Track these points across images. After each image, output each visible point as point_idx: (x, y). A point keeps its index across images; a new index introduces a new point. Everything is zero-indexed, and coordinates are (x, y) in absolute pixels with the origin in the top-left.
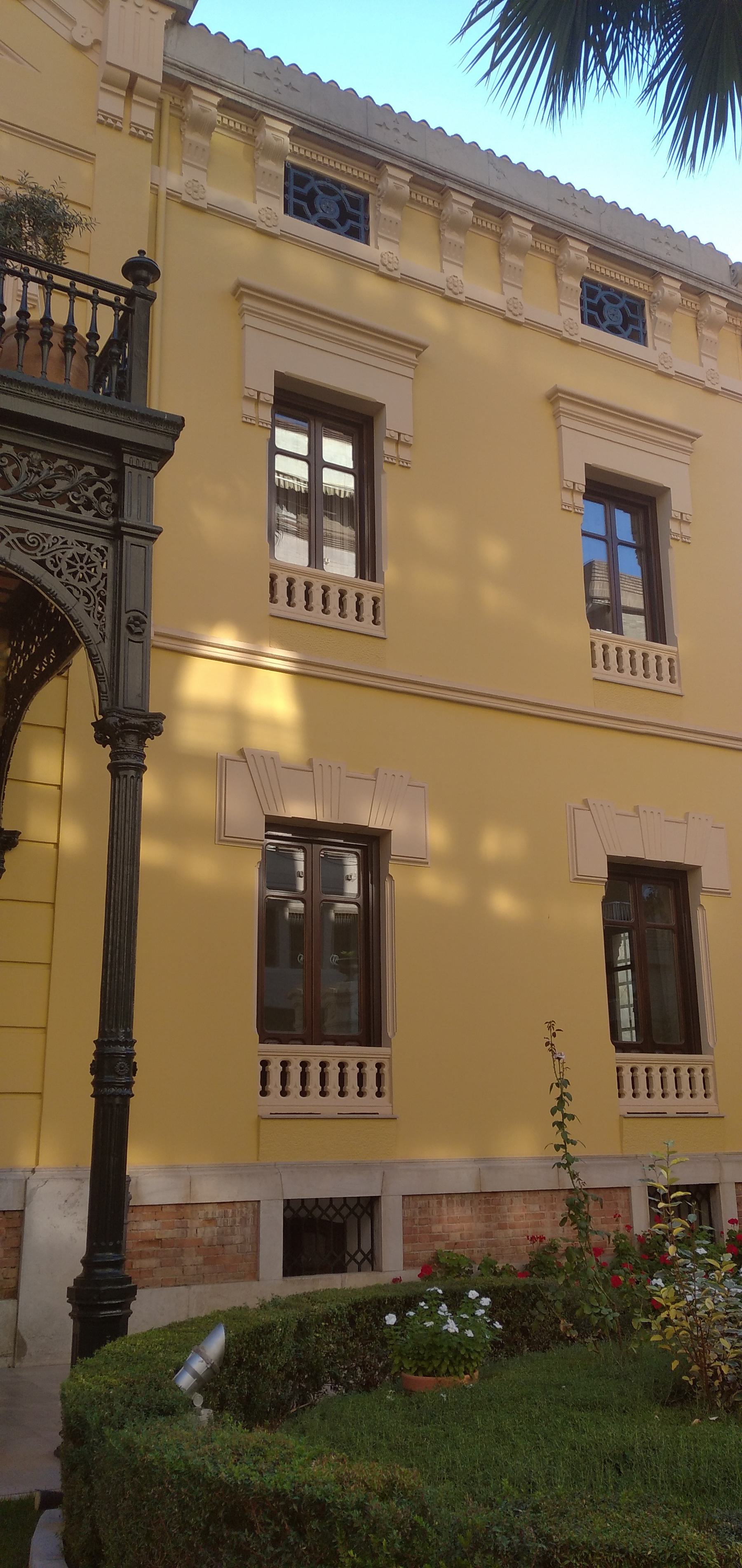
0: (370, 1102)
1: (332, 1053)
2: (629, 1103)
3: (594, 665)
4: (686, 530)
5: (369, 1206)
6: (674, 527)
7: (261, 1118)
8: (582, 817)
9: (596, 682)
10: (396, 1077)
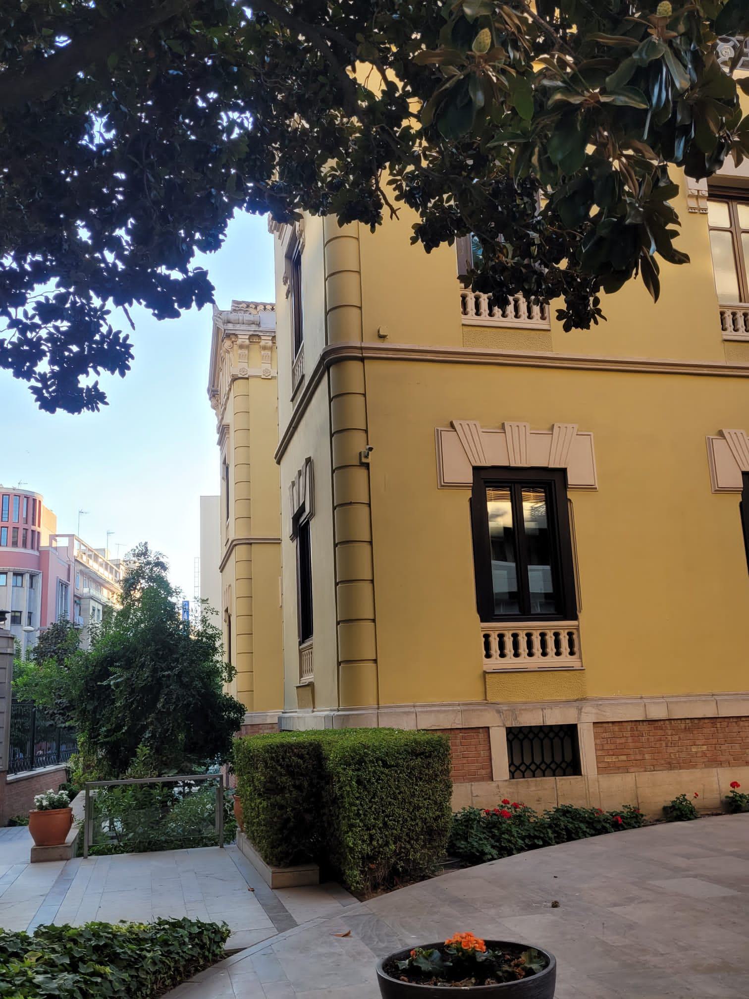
7: (485, 673)
8: (719, 444)
9: (726, 343)
10: (585, 641)
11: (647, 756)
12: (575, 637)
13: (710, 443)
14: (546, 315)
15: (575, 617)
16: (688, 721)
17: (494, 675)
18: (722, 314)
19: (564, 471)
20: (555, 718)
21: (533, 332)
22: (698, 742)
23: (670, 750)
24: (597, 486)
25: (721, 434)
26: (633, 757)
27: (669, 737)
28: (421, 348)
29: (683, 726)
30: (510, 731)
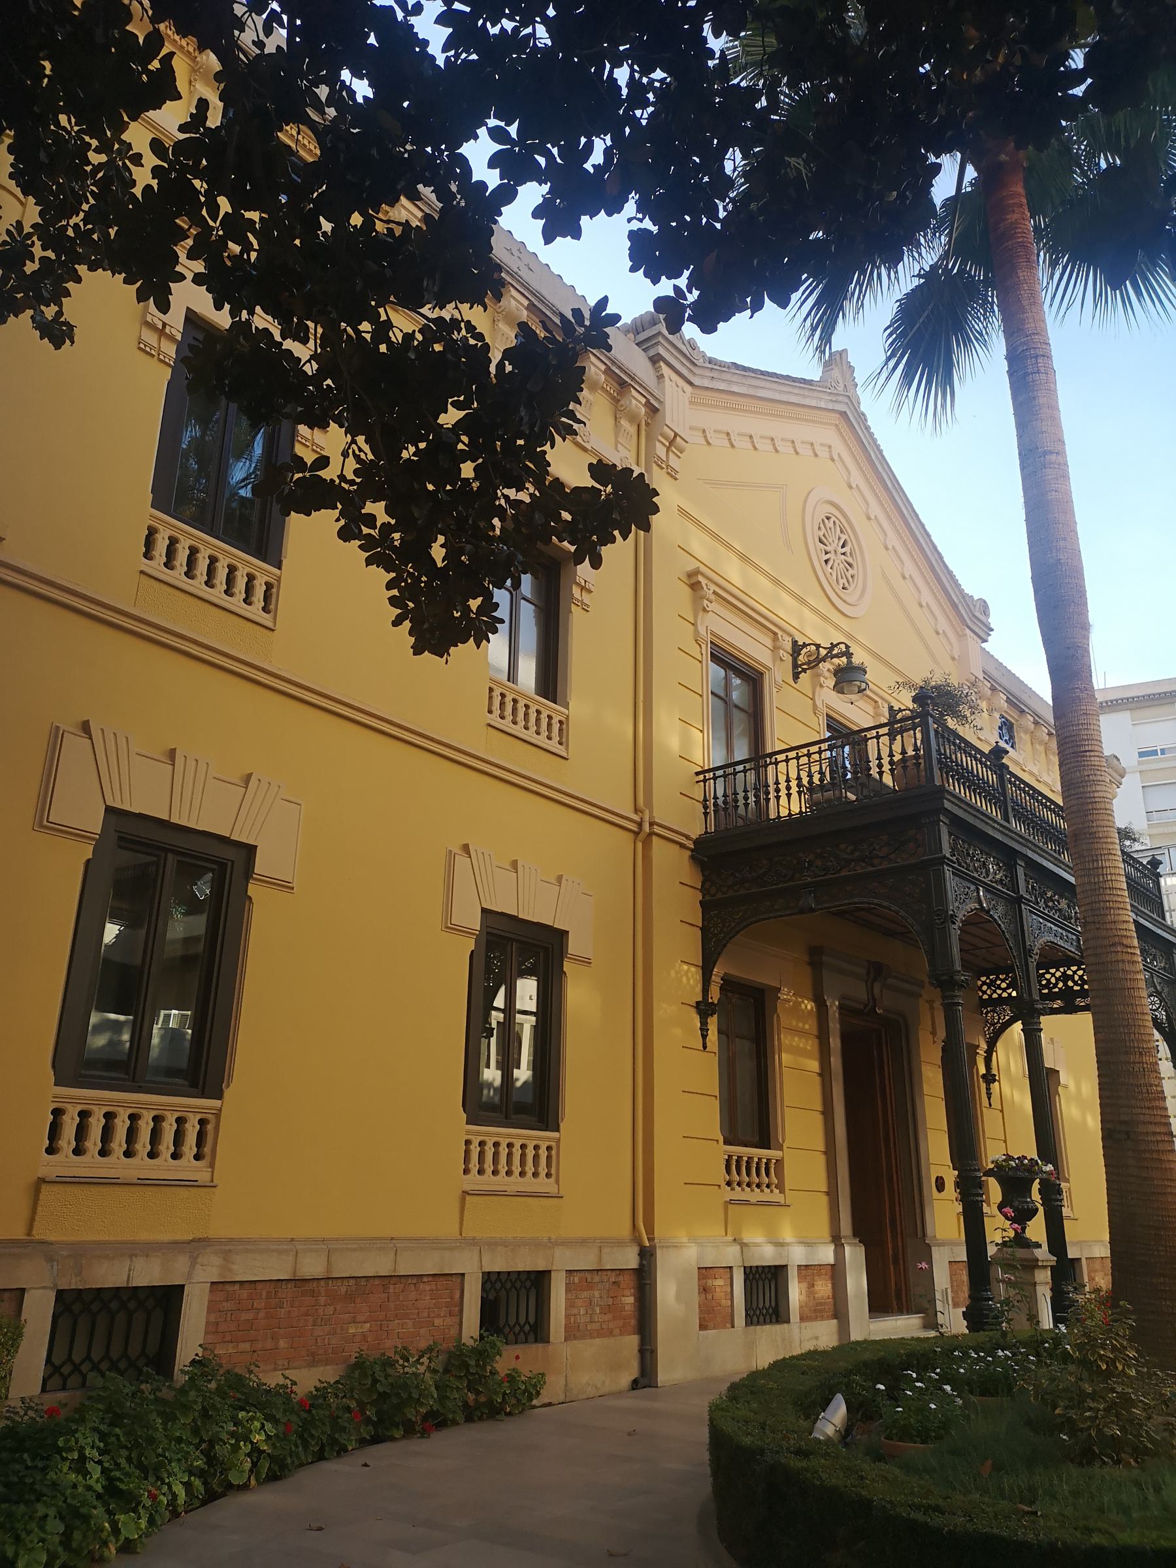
0: (188, 1168)
2: (473, 1181)
3: (490, 712)
4: (586, 598)
5: (1079, 1259)
6: (576, 591)
7: (42, 1181)
8: (461, 861)
11: (282, 1343)
12: (210, 1127)
14: (272, 607)
15: (219, 1096)
16: (352, 1282)
18: (491, 690)
19: (251, 850)
22: (360, 1318)
23: (318, 1331)
24: (294, 885)
25: (466, 848)
26: (259, 1345)
29: (343, 1290)
30: (60, 1294)
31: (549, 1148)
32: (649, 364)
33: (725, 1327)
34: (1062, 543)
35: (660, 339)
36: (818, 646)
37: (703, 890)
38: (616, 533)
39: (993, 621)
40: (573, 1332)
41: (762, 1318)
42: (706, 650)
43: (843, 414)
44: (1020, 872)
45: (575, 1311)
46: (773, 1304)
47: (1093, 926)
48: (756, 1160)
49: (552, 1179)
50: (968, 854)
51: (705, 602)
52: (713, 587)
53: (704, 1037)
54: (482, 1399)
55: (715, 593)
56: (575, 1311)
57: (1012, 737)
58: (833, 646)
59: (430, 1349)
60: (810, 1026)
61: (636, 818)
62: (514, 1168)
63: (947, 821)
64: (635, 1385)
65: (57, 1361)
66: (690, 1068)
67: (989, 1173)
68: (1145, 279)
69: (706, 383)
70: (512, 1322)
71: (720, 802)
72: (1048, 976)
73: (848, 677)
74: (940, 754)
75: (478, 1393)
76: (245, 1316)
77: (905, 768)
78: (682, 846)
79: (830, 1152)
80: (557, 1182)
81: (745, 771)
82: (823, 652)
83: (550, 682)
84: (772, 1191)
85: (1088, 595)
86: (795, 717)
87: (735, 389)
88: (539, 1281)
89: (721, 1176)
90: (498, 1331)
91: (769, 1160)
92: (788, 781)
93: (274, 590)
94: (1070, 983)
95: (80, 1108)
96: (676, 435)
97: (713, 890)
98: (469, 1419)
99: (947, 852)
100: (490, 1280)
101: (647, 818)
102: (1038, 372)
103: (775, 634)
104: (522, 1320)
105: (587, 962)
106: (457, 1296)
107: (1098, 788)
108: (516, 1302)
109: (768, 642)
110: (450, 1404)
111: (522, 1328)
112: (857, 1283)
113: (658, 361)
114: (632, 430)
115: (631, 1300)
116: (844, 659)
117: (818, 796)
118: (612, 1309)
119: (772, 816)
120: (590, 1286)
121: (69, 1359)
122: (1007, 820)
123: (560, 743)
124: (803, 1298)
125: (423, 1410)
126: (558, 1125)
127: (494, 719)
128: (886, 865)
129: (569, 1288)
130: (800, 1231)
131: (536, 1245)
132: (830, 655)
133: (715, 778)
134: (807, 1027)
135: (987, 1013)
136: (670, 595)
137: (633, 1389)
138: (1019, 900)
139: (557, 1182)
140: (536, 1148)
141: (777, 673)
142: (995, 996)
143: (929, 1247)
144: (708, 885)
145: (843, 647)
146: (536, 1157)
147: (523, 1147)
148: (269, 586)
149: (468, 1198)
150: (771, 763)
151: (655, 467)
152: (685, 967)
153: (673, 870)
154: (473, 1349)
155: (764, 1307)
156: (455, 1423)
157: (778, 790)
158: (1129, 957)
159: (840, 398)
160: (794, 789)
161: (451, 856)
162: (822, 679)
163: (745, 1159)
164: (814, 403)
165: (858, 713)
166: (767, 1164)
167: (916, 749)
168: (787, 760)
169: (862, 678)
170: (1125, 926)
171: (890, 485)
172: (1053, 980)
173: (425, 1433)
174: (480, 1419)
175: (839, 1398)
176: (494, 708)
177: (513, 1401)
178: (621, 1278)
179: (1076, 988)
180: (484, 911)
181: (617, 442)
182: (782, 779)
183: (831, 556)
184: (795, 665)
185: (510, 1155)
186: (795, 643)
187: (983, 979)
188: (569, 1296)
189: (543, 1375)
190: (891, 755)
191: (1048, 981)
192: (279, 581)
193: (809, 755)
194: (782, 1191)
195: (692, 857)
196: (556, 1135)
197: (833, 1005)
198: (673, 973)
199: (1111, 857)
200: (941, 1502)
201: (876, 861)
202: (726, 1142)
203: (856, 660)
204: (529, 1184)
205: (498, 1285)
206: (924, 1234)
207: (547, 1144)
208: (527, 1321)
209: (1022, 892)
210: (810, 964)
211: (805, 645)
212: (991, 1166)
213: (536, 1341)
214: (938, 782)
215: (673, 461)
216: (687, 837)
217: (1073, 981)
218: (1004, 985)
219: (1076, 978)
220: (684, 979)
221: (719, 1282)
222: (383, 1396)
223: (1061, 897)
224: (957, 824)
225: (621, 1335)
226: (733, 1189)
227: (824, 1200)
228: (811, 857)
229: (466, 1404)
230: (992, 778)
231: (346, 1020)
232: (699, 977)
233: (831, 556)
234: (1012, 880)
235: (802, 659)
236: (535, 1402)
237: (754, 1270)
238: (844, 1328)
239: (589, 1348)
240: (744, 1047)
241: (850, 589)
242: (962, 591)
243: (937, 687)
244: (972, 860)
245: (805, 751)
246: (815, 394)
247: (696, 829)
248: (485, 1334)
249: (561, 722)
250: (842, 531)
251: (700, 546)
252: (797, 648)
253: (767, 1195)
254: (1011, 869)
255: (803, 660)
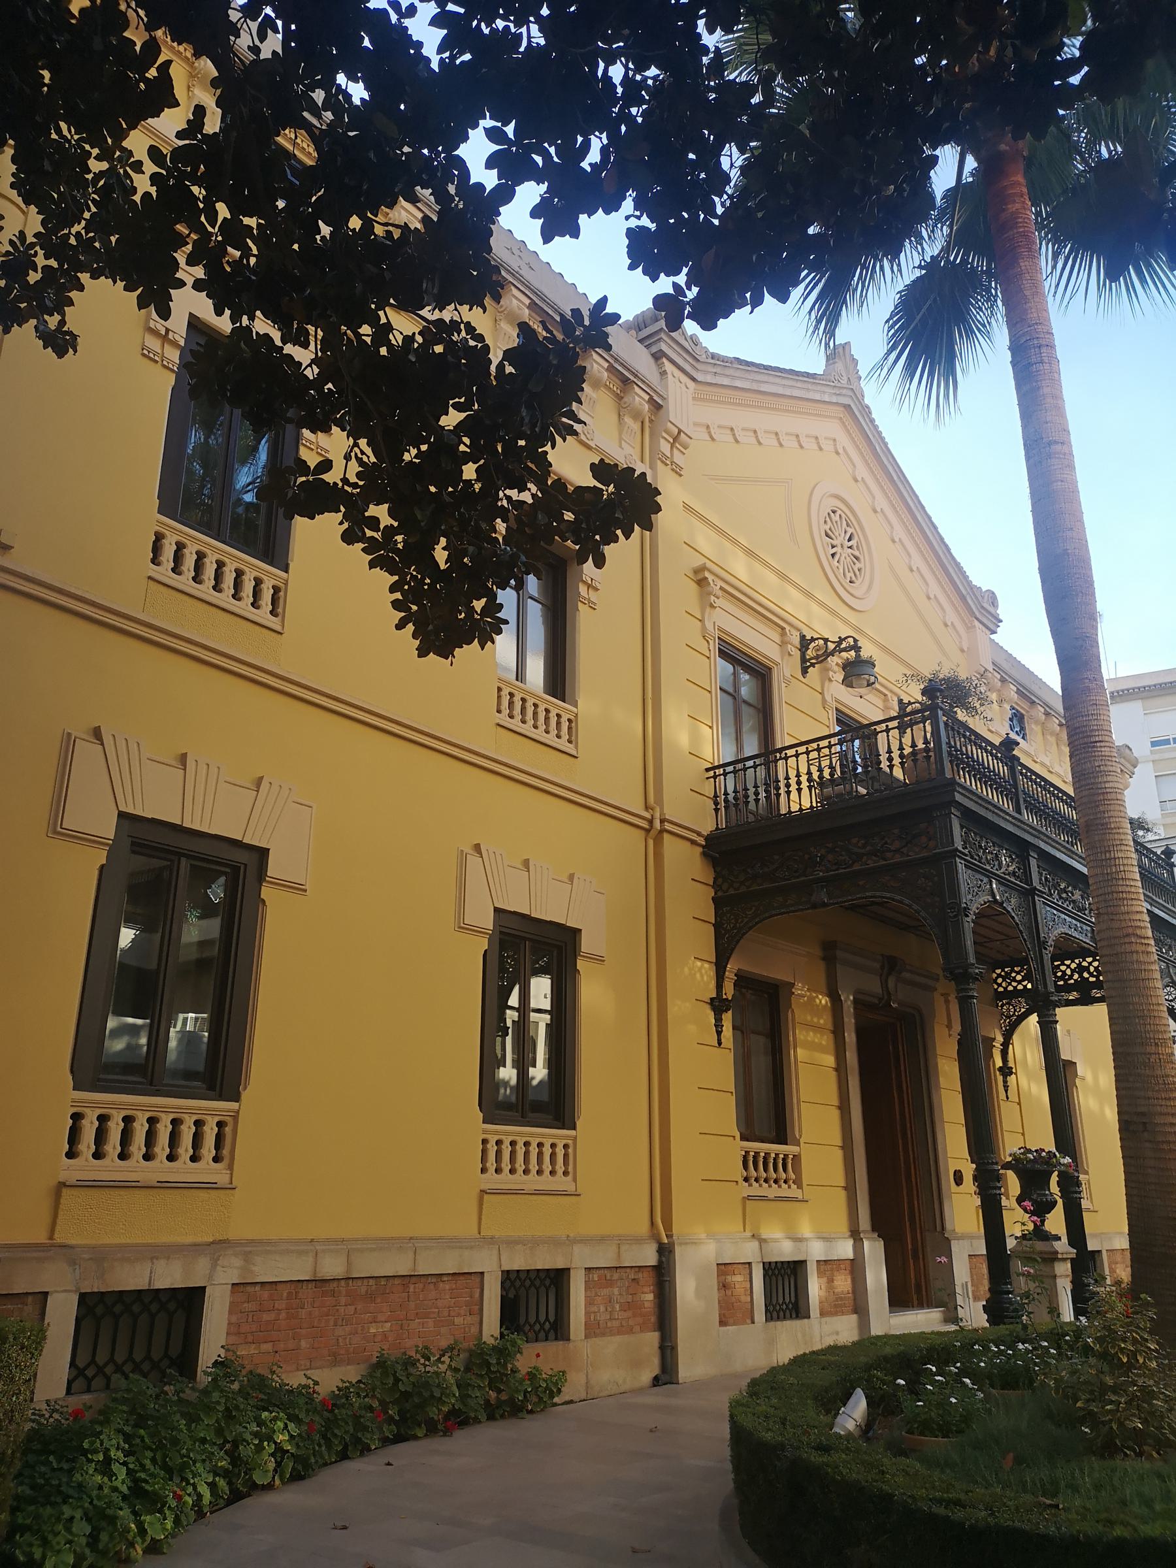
0: (207, 1171)
1: (167, 1106)
2: (491, 1180)
3: (499, 711)
4: (593, 596)
6: (583, 589)
7: (63, 1185)
8: (473, 861)
9: (499, 728)
11: (303, 1344)
12: (228, 1130)
13: (462, 858)
14: (280, 610)
15: (237, 1099)
16: (372, 1282)
17: (75, 1192)
18: (499, 689)
19: (263, 853)
20: (169, 1276)
21: (257, 628)
22: (381, 1317)
23: (339, 1331)
24: (307, 887)
25: (477, 848)
26: (282, 1346)
27: (342, 1309)
28: (73, 590)
29: (363, 1290)
30: (84, 1299)
31: (566, 1146)
32: (652, 361)
33: (744, 1323)
34: (1069, 534)
35: (663, 335)
36: (826, 640)
37: (716, 885)
38: (619, 532)
39: (1001, 612)
40: (593, 1330)
41: (781, 1314)
42: (714, 646)
43: (847, 407)
44: (1033, 863)
45: (595, 1309)
46: (793, 1300)
47: (1106, 917)
48: (773, 1155)
49: (570, 1178)
50: (980, 847)
51: (713, 598)
52: (720, 583)
53: (719, 1033)
54: (504, 1397)
55: (721, 588)
56: (595, 1309)
57: (1022, 729)
58: (841, 640)
59: (451, 1348)
60: (825, 1020)
61: (648, 815)
62: (531, 1167)
63: (958, 814)
64: (656, 1381)
65: (81, 1363)
66: (706, 1066)
67: (1007, 1166)
68: (1149, 266)
69: (709, 379)
70: (532, 1320)
71: (731, 797)
72: (1063, 968)
73: (857, 670)
74: (950, 747)
75: (499, 1391)
76: (266, 1317)
77: (915, 761)
78: (693, 842)
79: (847, 1146)
80: (575, 1180)
81: (755, 766)
82: (831, 646)
83: (559, 680)
84: (789, 1187)
85: (1096, 585)
86: (805, 712)
87: (738, 384)
88: (558, 1279)
89: (740, 1172)
90: (519, 1330)
91: (786, 1156)
92: (798, 776)
93: (282, 594)
94: (1086, 975)
95: (98, 1112)
96: (680, 431)
97: (725, 886)
98: (491, 1417)
99: (959, 844)
100: (510, 1279)
101: (657, 815)
102: (1042, 362)
103: (783, 629)
104: (542, 1318)
105: (600, 960)
106: (477, 1295)
107: (1109, 778)
108: (535, 1300)
109: (777, 638)
110: (472, 1403)
111: (542, 1326)
112: (876, 1277)
113: (660, 358)
114: (636, 427)
115: (650, 1297)
116: (853, 653)
117: (828, 791)
118: (631, 1306)
119: (783, 811)
120: (610, 1283)
121: (93, 1361)
122: (1019, 812)
123: (570, 741)
124: (823, 1293)
125: (445, 1409)
126: (575, 1124)
127: (503, 718)
128: (898, 858)
129: (588, 1285)
130: (819, 1227)
131: (554, 1242)
132: (838, 649)
133: (725, 774)
134: (822, 1021)
135: (1002, 1006)
136: (677, 594)
137: (654, 1386)
138: (1033, 892)
139: (575, 1180)
140: (553, 1146)
141: (785, 668)
142: (1010, 988)
143: (948, 1241)
144: (720, 880)
145: (851, 640)
146: (553, 1156)
147: (540, 1145)
148: (276, 590)
149: (486, 1197)
150: (781, 758)
151: (659, 462)
152: (699, 964)
153: (685, 865)
154: (494, 1348)
155: (784, 1302)
156: (477, 1421)
157: (788, 785)
158: (1143, 948)
159: (844, 391)
160: (805, 784)
161: (462, 858)
162: (831, 673)
163: (762, 1154)
164: (817, 397)
165: (867, 707)
166: (784, 1159)
167: (926, 742)
168: (797, 755)
169: (869, 670)
170: (1138, 917)
171: (895, 478)
172: (1069, 972)
173: (447, 1432)
174: (502, 1417)
175: (859, 1391)
176: (503, 708)
177: (535, 1399)
178: (640, 1275)
179: (1092, 979)
180: (497, 910)
181: (621, 439)
182: (792, 774)
183: (838, 549)
184: (804, 660)
185: (527, 1154)
186: (803, 637)
187: (998, 971)
188: (589, 1294)
189: (564, 1372)
190: (901, 748)
191: (1064, 972)
192: (286, 584)
193: (819, 750)
194: (800, 1187)
195: (704, 854)
196: (572, 1133)
197: (848, 999)
198: (686, 970)
199: (1123, 848)
200: (962, 1496)
201: (889, 855)
202: (743, 1138)
203: (864, 654)
204: (546, 1182)
205: (518, 1283)
206: (943, 1228)
207: (564, 1142)
208: (547, 1319)
209: (1036, 883)
210: (824, 959)
211: (813, 640)
212: (1009, 1159)
213: (556, 1339)
214: (948, 775)
215: (678, 457)
216: (699, 834)
217: (1089, 973)
218: (1019, 978)
219: (1092, 969)
220: (698, 975)
221: (738, 1278)
222: (406, 1395)
223: (1075, 888)
224: (969, 816)
225: (642, 1331)
226: (750, 1185)
227: (842, 1195)
228: (823, 851)
229: (487, 1402)
230: (1003, 770)
231: (359, 1020)
232: (713, 973)
233: (838, 549)
234: (1025, 872)
235: (810, 653)
236: (556, 1400)
237: (773, 1266)
238: (864, 1323)
239: (611, 1345)
240: (759, 1043)
241: (858, 583)
242: (969, 583)
243: (947, 680)
244: (984, 852)
245: (814, 745)
246: (819, 388)
247: (708, 826)
248: (506, 1332)
249: (569, 720)
250: (848, 525)
251: (706, 542)
252: (805, 643)
253: (784, 1191)
254: (1024, 861)
255: (811, 654)
